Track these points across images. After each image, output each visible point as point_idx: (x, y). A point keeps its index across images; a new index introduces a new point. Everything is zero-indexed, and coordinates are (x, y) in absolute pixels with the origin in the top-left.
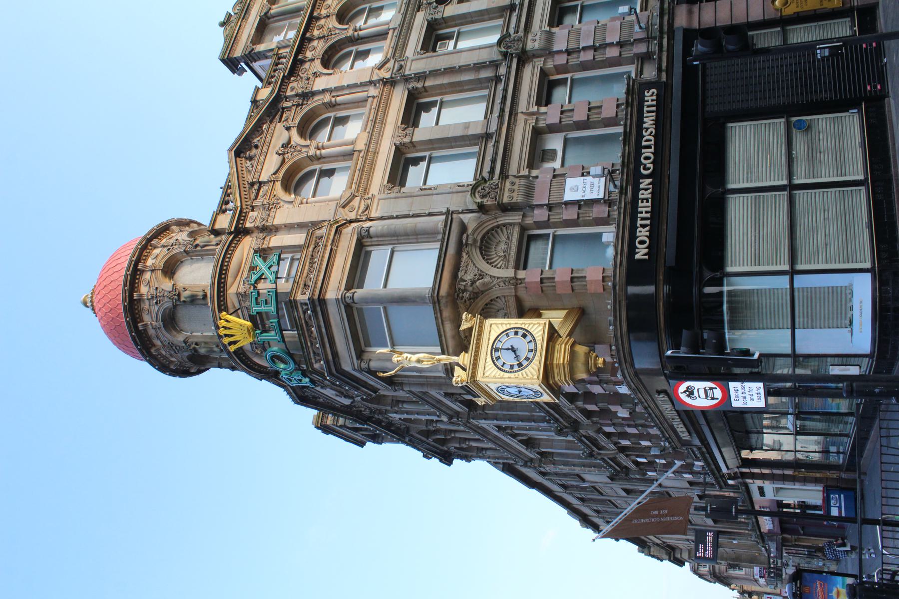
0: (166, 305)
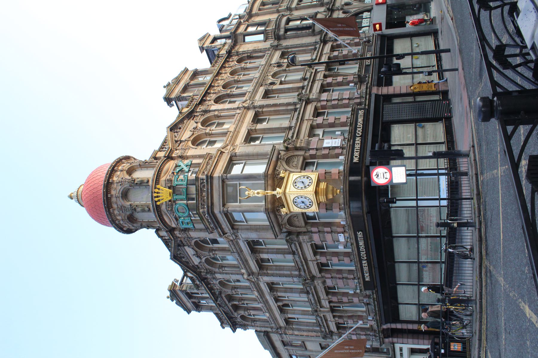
0: (125, 186)
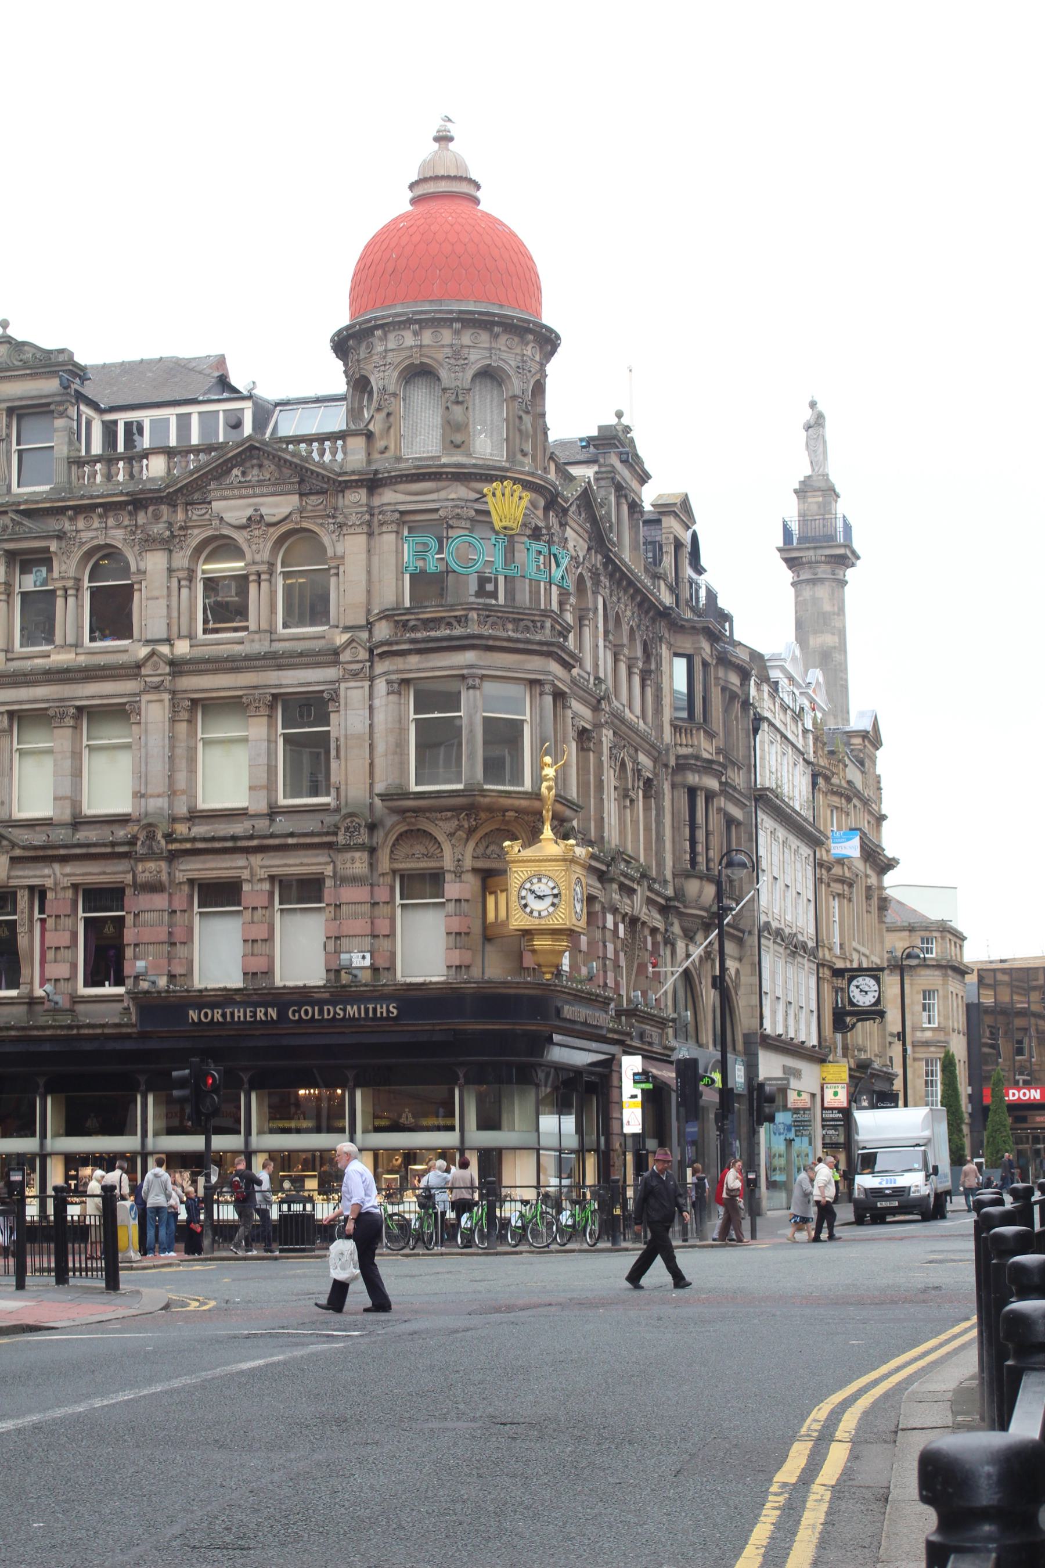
0: (515, 381)
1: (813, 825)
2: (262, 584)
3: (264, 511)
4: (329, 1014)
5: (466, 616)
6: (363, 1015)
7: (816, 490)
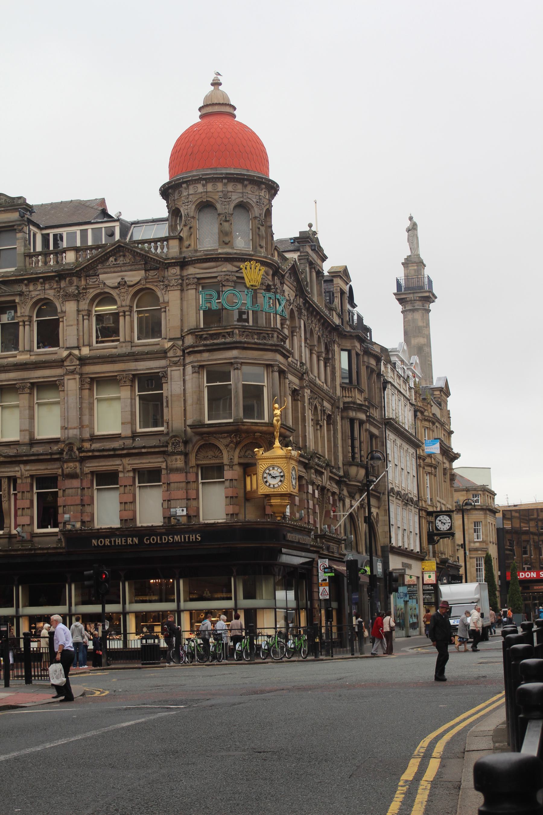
1: (415, 437)
2: (127, 317)
3: (126, 279)
4: (165, 540)
5: (233, 332)
6: (183, 540)
7: (414, 263)
